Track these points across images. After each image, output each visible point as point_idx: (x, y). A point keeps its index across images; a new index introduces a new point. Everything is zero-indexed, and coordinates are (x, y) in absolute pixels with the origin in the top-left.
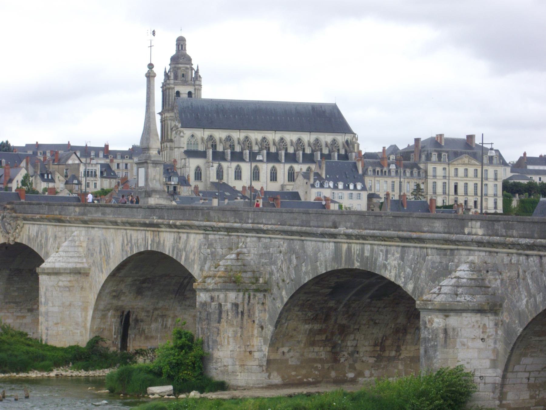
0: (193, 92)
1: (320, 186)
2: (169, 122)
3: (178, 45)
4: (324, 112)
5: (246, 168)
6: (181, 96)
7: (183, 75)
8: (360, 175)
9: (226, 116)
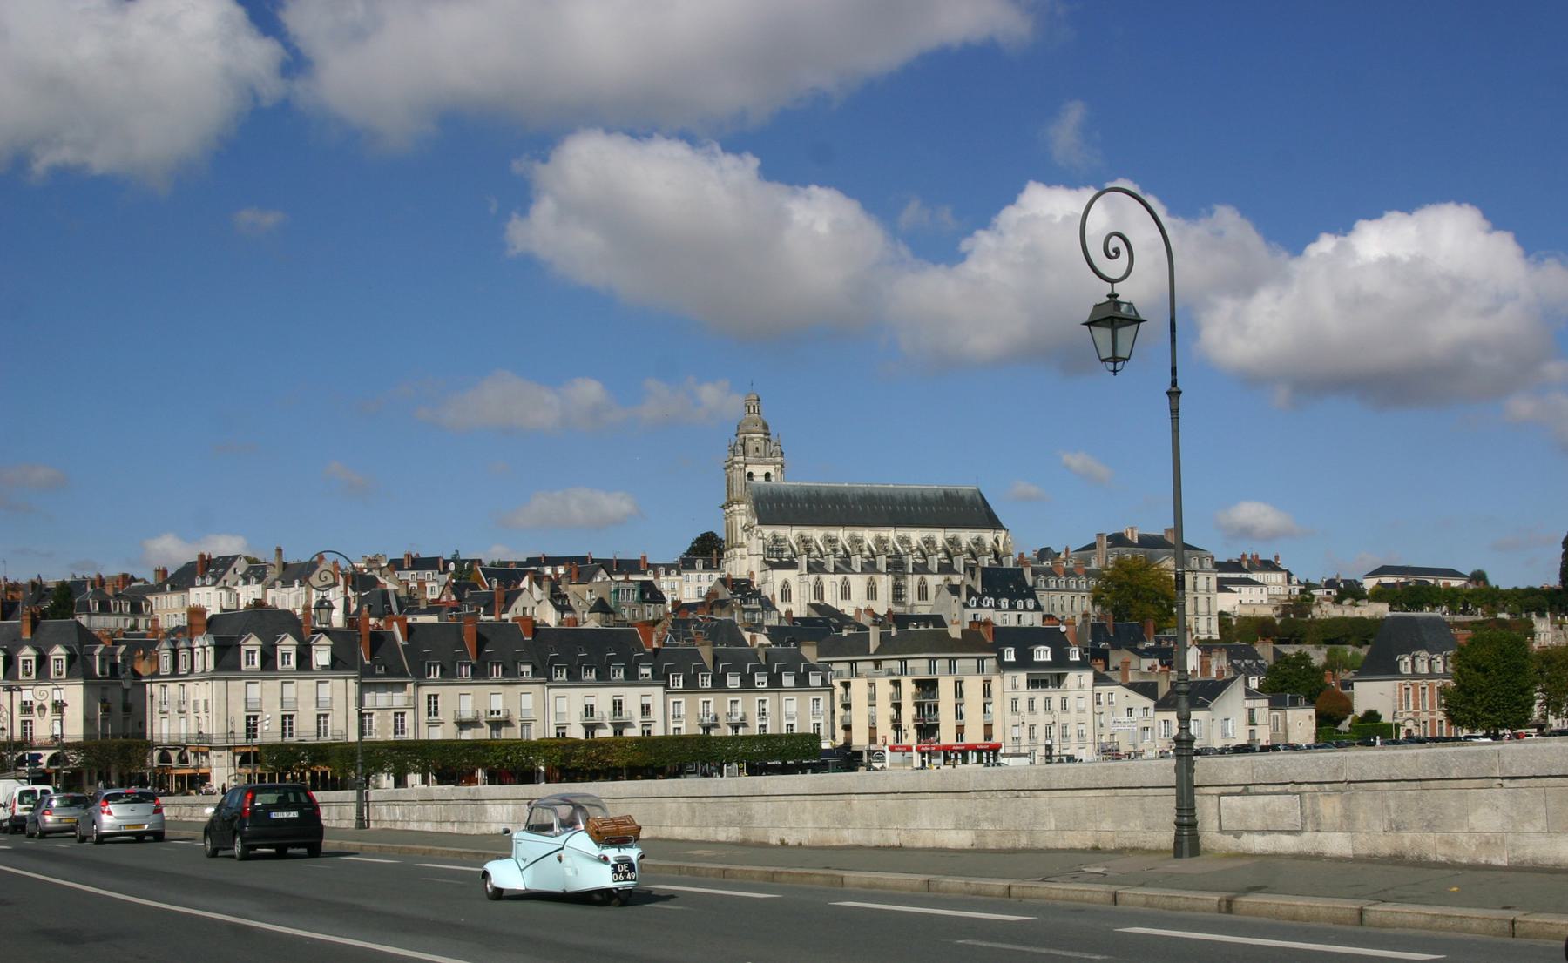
0: (772, 473)
2: (738, 518)
5: (858, 583)
6: (755, 479)
7: (757, 448)
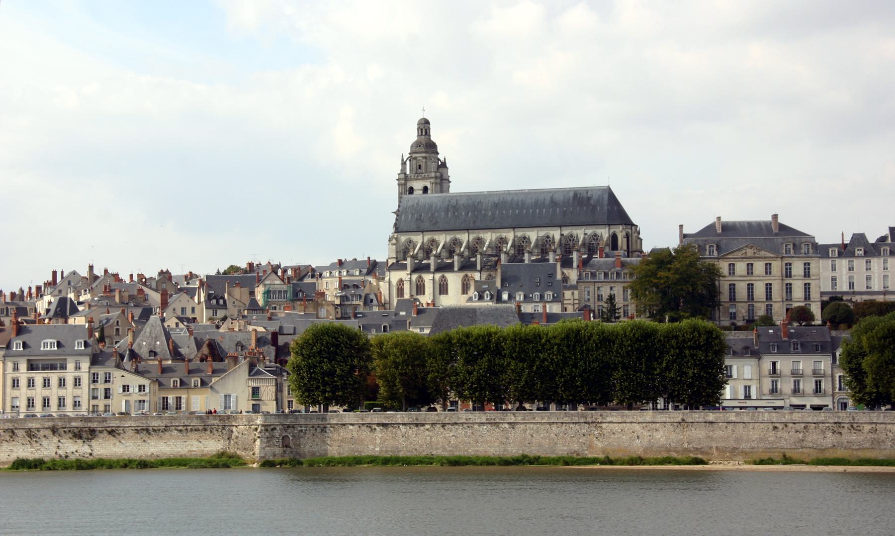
1: (479, 299)
3: (420, 130)
4: (589, 199)
5: (454, 280)
7: (420, 166)
8: (558, 281)
9: (456, 214)
